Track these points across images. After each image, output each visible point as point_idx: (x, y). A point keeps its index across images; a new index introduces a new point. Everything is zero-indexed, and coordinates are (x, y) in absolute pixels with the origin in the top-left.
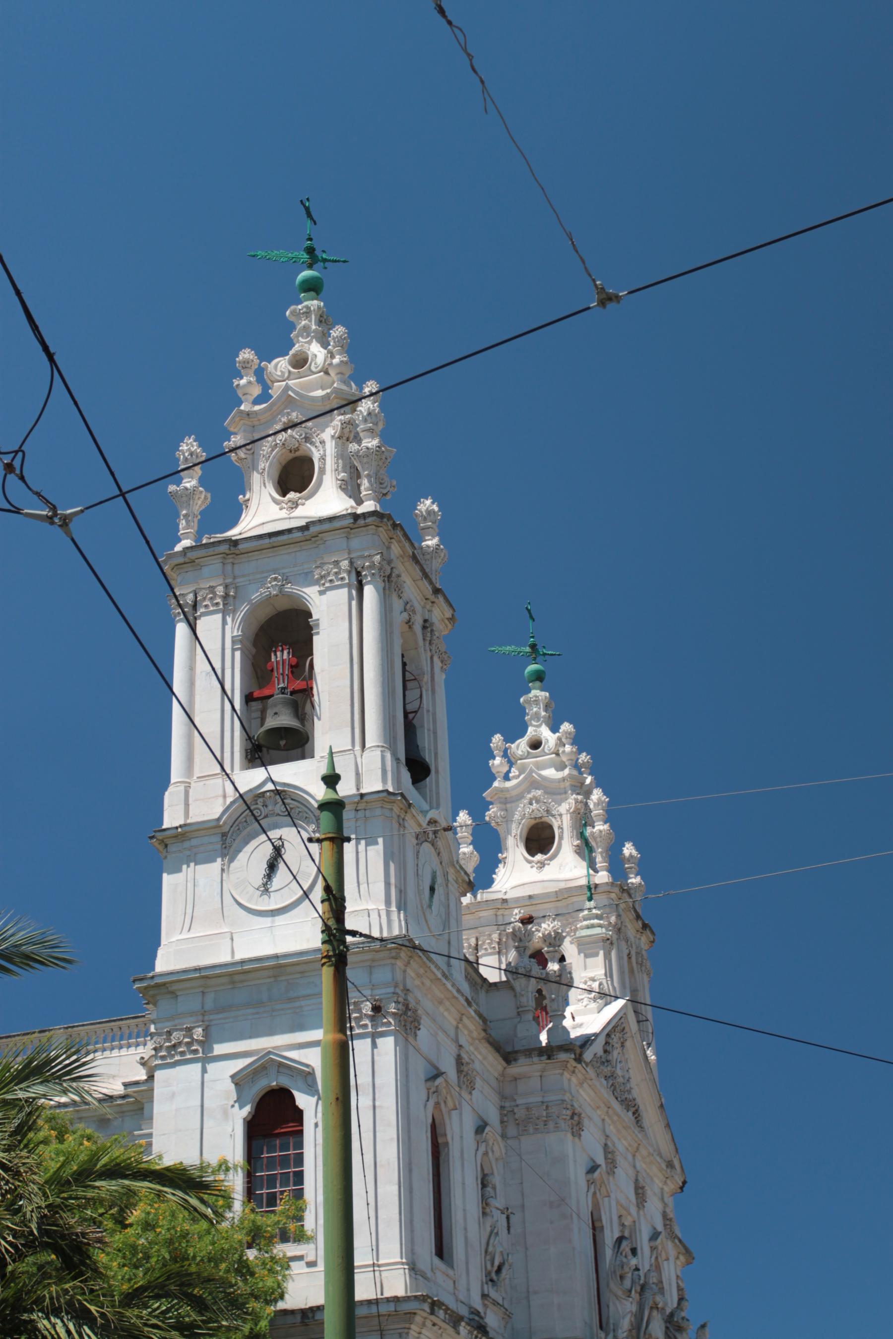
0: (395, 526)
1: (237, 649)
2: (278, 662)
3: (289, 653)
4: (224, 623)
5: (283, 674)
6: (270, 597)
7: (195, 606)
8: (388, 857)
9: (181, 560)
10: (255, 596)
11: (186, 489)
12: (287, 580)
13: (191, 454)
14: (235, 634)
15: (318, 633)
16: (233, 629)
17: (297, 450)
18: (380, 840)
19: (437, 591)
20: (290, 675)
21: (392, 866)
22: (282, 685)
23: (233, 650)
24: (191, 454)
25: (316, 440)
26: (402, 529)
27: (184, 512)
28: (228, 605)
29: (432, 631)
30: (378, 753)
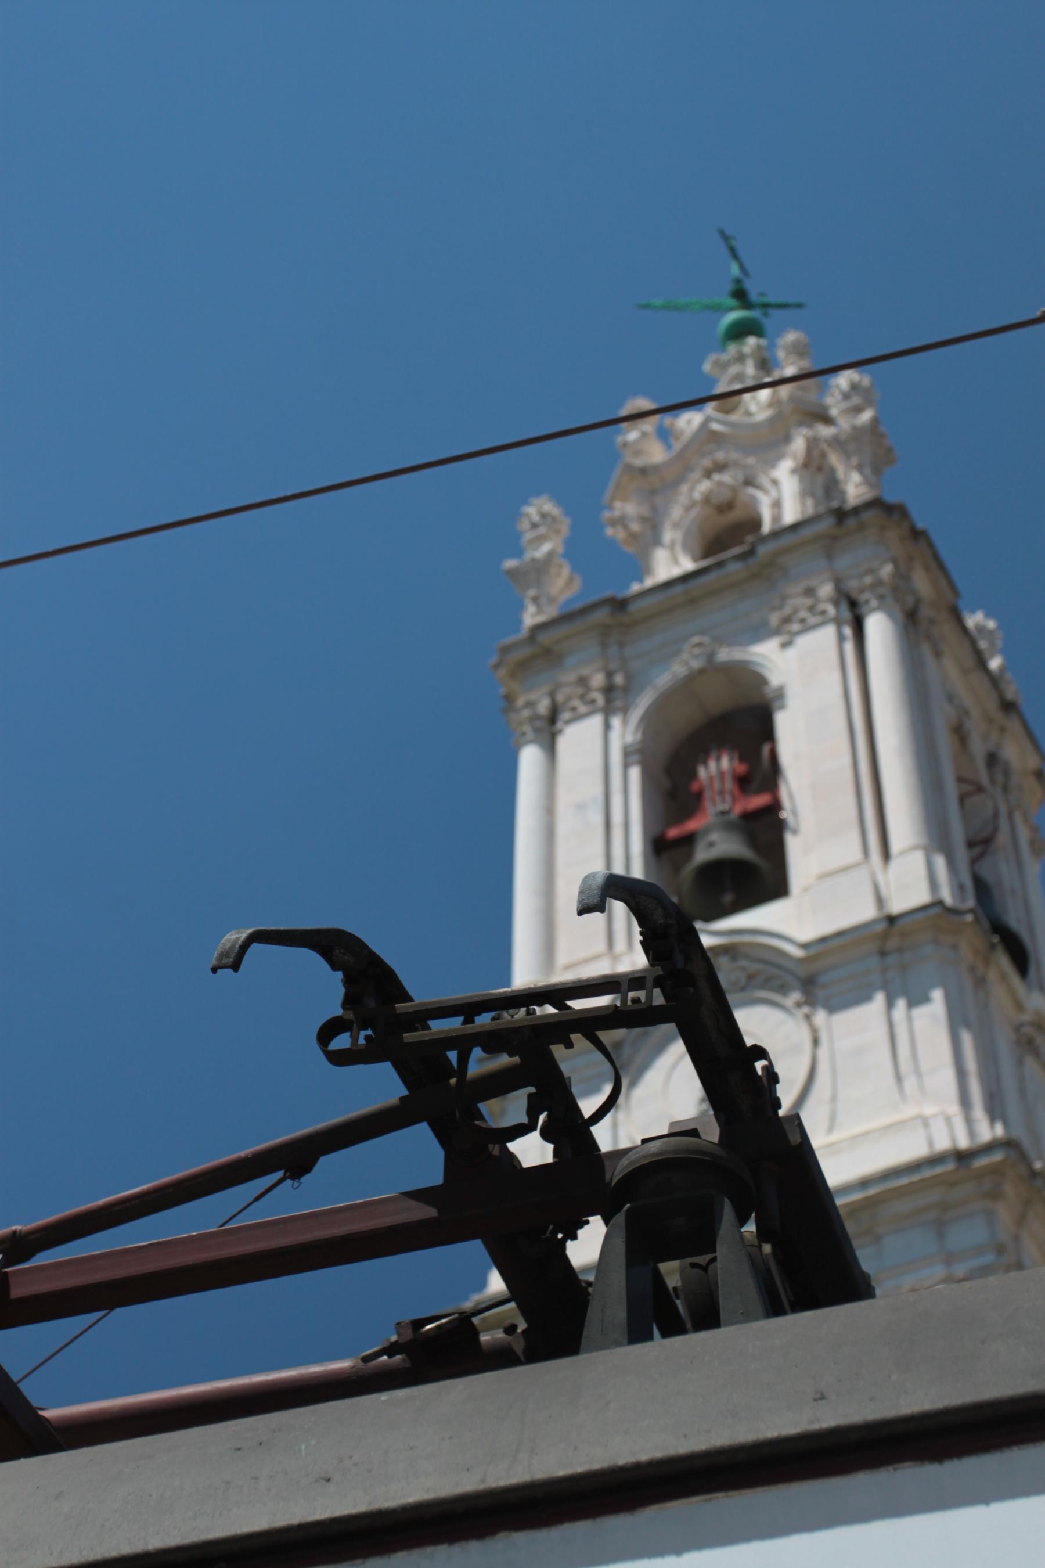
0: (917, 535)
1: (632, 764)
2: (711, 778)
3: (731, 759)
4: (607, 727)
6: (687, 685)
7: (553, 717)
8: (956, 1021)
9: (525, 652)
10: (665, 678)
11: (533, 560)
13: (544, 516)
14: (630, 739)
15: (782, 707)
18: (937, 995)
19: (1008, 707)
20: (737, 792)
21: (967, 1039)
23: (626, 766)
25: (764, 481)
26: (930, 545)
27: (532, 592)
29: (1007, 773)
30: (918, 859)
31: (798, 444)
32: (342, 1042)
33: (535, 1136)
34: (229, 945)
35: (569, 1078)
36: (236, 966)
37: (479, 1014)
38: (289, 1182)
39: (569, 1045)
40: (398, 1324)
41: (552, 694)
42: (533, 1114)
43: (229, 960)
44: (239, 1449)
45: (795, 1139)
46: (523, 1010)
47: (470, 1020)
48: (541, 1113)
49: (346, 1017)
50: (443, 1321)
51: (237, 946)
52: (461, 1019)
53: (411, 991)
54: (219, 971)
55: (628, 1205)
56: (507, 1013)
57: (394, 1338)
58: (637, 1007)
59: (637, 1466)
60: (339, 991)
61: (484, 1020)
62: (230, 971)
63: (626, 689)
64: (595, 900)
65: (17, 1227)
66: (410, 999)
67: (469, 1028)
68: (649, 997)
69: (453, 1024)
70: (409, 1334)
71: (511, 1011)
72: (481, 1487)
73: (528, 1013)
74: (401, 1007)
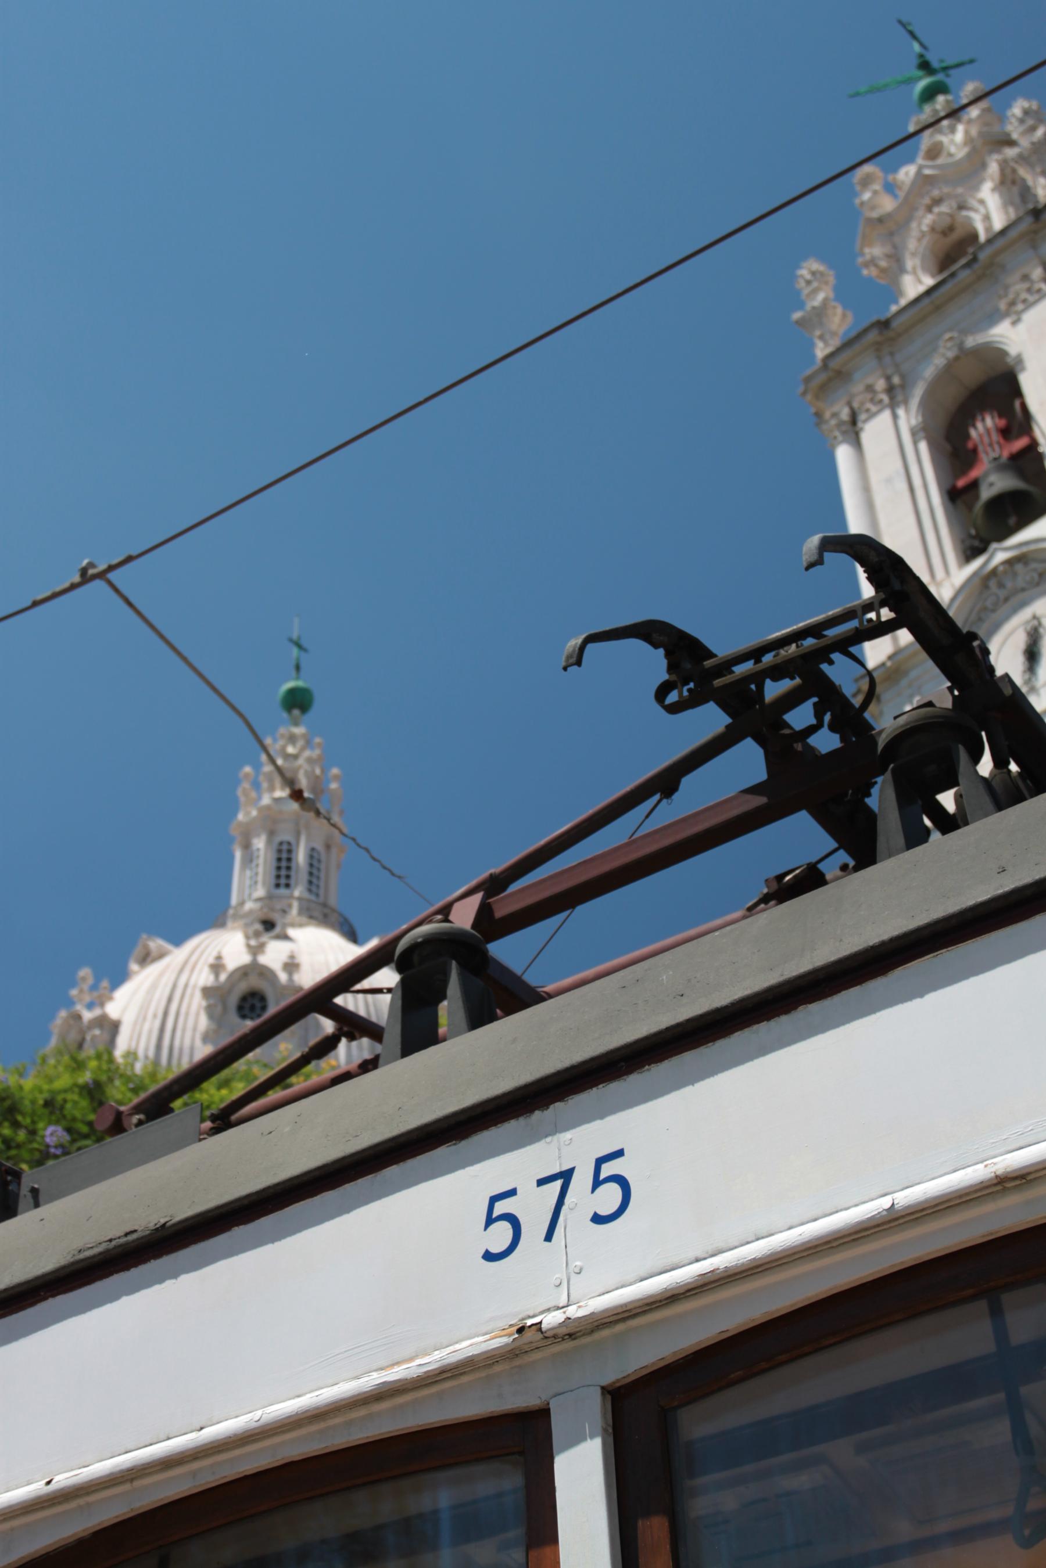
1: (919, 440)
2: (980, 436)
3: (993, 418)
4: (895, 417)
5: (991, 445)
6: (948, 371)
7: (854, 421)
9: (823, 377)
10: (929, 371)
11: (814, 308)
12: (965, 332)
13: (813, 273)
14: (913, 422)
15: (1023, 369)
16: (909, 418)
17: (951, 229)
20: (1002, 441)
22: (993, 455)
23: (915, 443)
24: (813, 273)
25: (974, 203)
27: (818, 333)
28: (895, 396)
31: (993, 168)
32: (673, 697)
33: (825, 731)
34: (571, 649)
35: (840, 686)
36: (579, 663)
37: (763, 655)
38: (665, 801)
39: (831, 662)
40: (766, 880)
41: (849, 404)
42: (819, 714)
43: (573, 660)
44: (624, 987)
45: (1008, 691)
46: (794, 646)
47: (758, 661)
48: (825, 714)
49: (672, 679)
50: (797, 872)
51: (577, 649)
52: (752, 662)
53: (714, 649)
54: (569, 669)
55: (892, 766)
56: (783, 650)
57: (765, 891)
58: (871, 625)
59: (883, 944)
60: (664, 663)
61: (768, 658)
62: (576, 667)
63: (903, 386)
64: (814, 558)
65: (492, 871)
66: (714, 656)
67: (760, 666)
68: (878, 615)
69: (745, 668)
70: (775, 886)
71: (786, 648)
72: (781, 979)
73: (797, 646)
74: (708, 663)
